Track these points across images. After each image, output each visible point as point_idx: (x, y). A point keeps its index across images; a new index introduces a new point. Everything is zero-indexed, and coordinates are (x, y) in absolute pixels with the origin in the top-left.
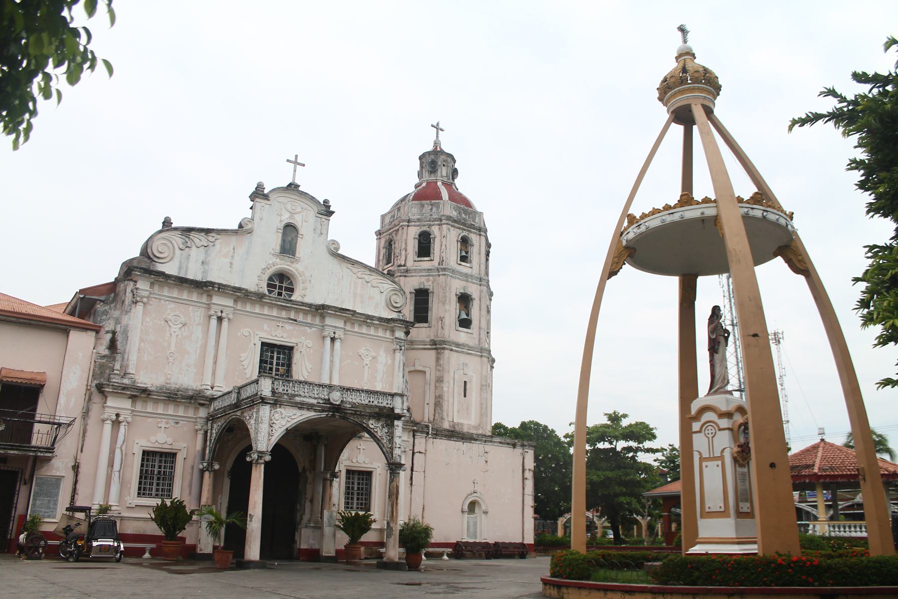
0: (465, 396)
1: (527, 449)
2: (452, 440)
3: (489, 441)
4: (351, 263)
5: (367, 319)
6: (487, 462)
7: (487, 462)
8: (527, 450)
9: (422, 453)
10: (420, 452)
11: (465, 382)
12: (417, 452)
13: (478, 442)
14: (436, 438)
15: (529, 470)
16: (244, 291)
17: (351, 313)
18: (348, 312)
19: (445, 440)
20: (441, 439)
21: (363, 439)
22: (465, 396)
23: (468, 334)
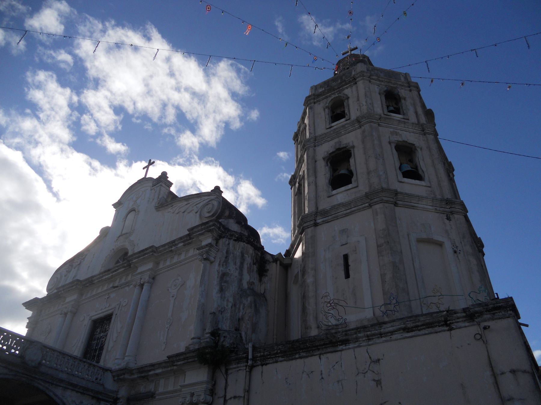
0: (347, 276)
1: (485, 321)
2: (296, 359)
3: (374, 335)
4: (169, 206)
5: (171, 247)
6: (378, 382)
7: (378, 382)
8: (486, 324)
9: (239, 397)
10: (235, 397)
11: (346, 257)
12: (231, 398)
13: (351, 346)
14: (266, 364)
15: (513, 372)
16: (76, 283)
17: (150, 250)
18: (148, 251)
19: (285, 362)
20: (277, 362)
21: (157, 397)
22: (347, 276)
23: (349, 192)
